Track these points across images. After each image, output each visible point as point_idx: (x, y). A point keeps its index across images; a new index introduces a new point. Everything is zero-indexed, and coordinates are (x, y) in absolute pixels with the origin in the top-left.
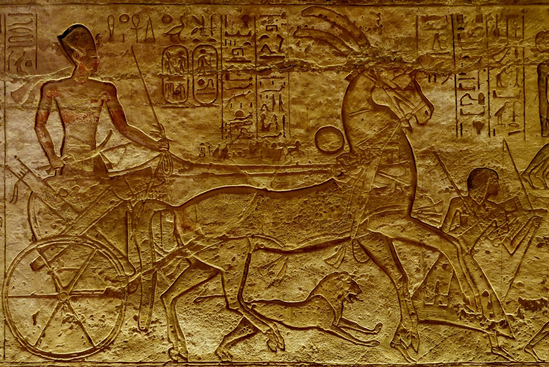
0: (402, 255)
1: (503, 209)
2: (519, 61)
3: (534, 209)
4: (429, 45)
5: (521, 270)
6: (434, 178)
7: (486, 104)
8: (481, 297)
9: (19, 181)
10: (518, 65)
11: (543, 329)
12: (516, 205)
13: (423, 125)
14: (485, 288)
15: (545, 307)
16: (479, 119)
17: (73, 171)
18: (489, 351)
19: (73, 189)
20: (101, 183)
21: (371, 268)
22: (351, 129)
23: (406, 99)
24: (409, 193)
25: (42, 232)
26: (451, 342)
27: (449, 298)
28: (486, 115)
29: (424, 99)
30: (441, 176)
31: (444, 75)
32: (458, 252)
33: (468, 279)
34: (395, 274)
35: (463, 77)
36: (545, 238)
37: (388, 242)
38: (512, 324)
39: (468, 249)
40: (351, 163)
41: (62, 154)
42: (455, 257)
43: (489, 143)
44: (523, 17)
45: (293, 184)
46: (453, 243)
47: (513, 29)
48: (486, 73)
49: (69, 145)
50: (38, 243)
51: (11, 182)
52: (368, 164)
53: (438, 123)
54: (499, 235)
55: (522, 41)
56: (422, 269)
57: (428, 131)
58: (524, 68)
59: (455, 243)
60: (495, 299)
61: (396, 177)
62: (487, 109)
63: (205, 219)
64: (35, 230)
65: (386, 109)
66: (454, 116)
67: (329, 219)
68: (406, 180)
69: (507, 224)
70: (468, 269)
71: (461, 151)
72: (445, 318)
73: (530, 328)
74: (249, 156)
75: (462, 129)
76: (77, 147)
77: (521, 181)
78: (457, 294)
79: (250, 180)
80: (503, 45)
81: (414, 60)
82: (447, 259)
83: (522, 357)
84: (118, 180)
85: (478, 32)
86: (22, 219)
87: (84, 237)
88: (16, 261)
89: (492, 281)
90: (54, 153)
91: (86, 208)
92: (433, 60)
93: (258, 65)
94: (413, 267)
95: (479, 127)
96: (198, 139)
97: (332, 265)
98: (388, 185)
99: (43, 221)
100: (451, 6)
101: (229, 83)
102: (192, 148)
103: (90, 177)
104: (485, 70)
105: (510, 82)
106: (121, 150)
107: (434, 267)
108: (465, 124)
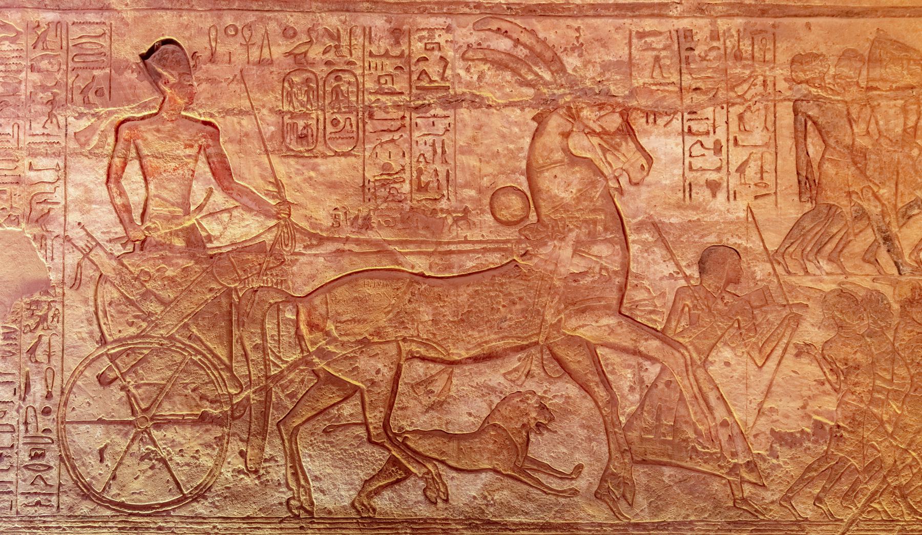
0: (610, 368)
3: (791, 303)
8: (719, 428)
9: (83, 258)
11: (804, 474)
12: (765, 298)
13: (637, 184)
17: (159, 245)
19: (158, 270)
20: (196, 263)
21: (568, 385)
22: (540, 190)
23: (616, 148)
24: (617, 280)
25: (113, 331)
29: (641, 149)
30: (663, 256)
32: (686, 366)
33: (701, 402)
34: (601, 392)
36: (806, 344)
37: (590, 348)
38: (762, 466)
40: (538, 237)
41: (142, 221)
43: (728, 211)
45: (460, 267)
46: (679, 352)
49: (152, 209)
50: (109, 347)
51: (73, 259)
52: (562, 239)
56: (638, 388)
59: (683, 351)
60: (738, 431)
61: (600, 257)
63: (339, 314)
64: (104, 327)
65: (589, 163)
67: (509, 316)
68: (615, 261)
70: (700, 389)
71: (690, 221)
72: (670, 456)
74: (400, 226)
75: (691, 190)
76: (164, 211)
77: (772, 264)
78: (686, 422)
79: (401, 259)
83: (776, 513)
84: (220, 259)
86: (87, 312)
87: (171, 338)
88: (77, 372)
89: (734, 405)
90: (132, 221)
91: (176, 298)
93: (412, 98)
94: (625, 385)
96: (332, 201)
97: (513, 381)
98: (590, 268)
99: (116, 315)
101: (373, 124)
102: (323, 217)
103: (181, 253)
106: (225, 217)
107: (654, 384)
108: (696, 184)
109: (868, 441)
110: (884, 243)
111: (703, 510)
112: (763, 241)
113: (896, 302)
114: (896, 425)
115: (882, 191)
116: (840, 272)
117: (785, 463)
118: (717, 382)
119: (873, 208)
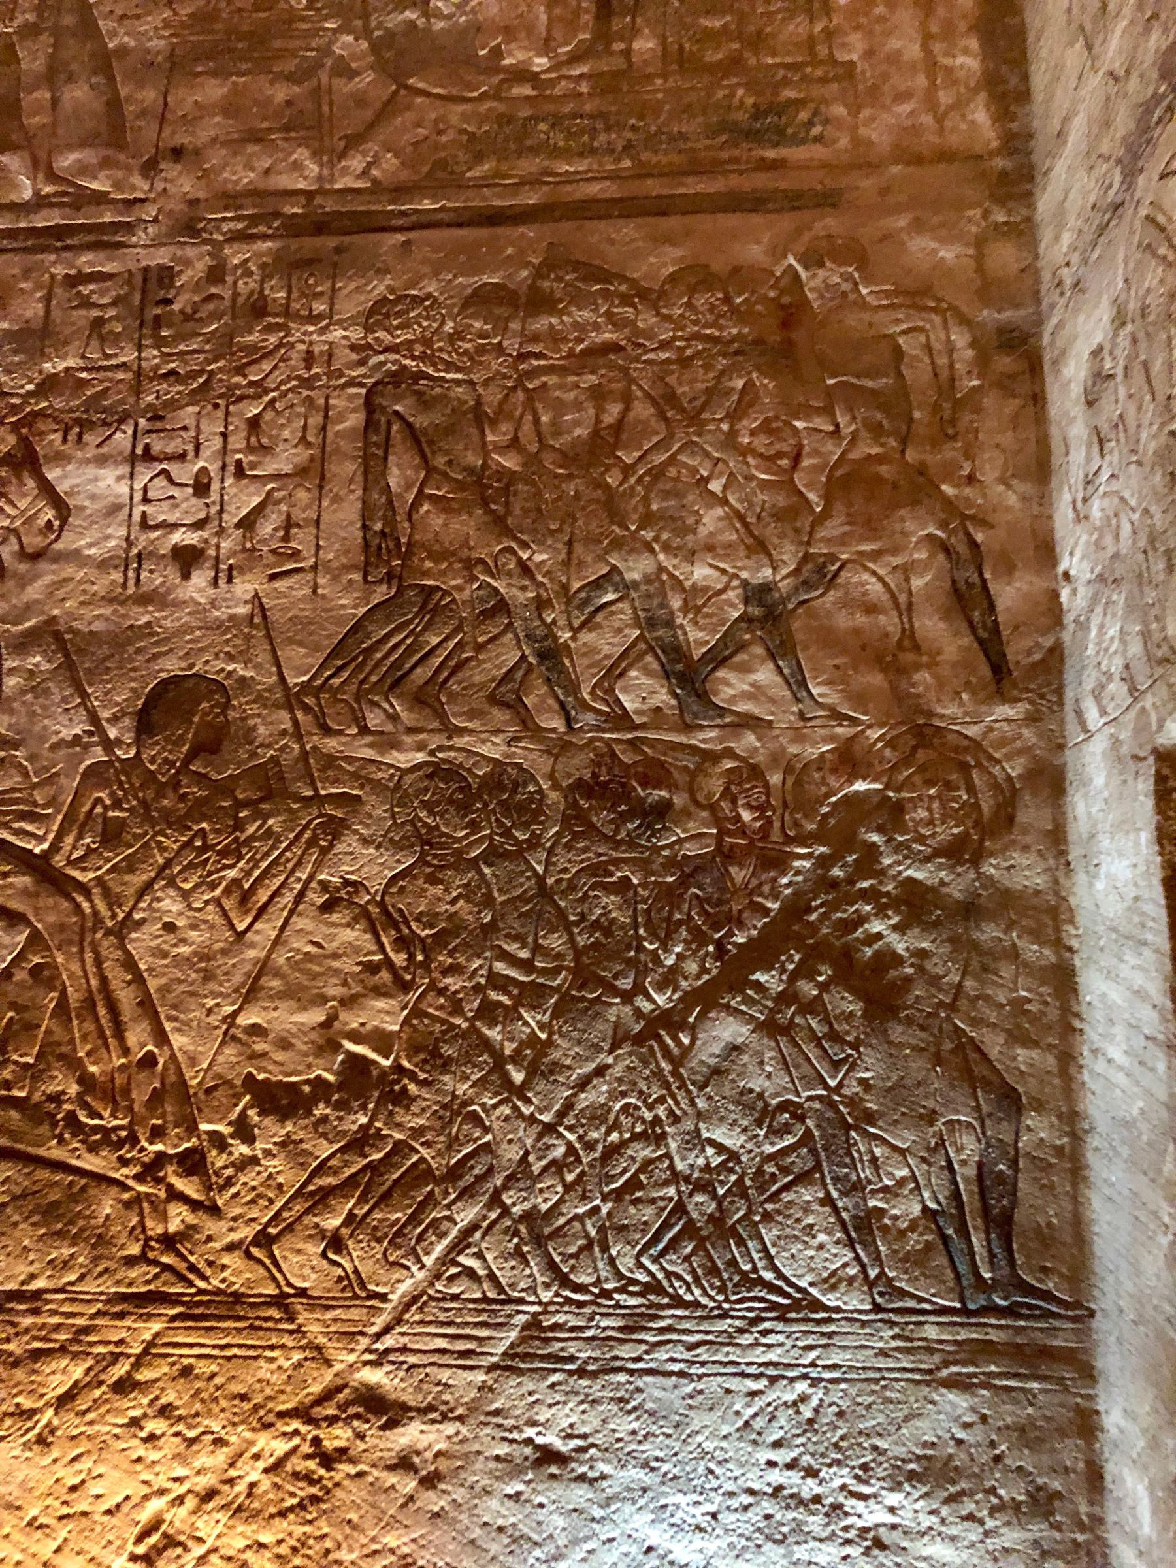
1: (231, 794)
2: (317, 377)
4: (75, 346)
5: (263, 981)
6: (45, 708)
7: (214, 496)
8: (134, 1070)
10: (312, 389)
13: (36, 556)
14: (150, 1040)
15: (321, 1105)
16: (192, 538)
18: (135, 1249)
26: (16, 1218)
27: (35, 1073)
28: (213, 527)
29: (47, 490)
30: (65, 700)
31: (105, 423)
33: (102, 1011)
35: (159, 425)
36: (347, 883)
39: (114, 916)
42: (70, 942)
44: (335, 265)
47: (303, 295)
48: (220, 414)
53: (77, 552)
54: (210, 874)
55: (327, 327)
57: (48, 574)
58: (327, 398)
59: (80, 899)
62: (214, 509)
66: (123, 532)
69: (236, 839)
70: (104, 981)
73: (270, 1176)
77: (292, 711)
78: (62, 1057)
80: (273, 340)
81: (30, 387)
82: (49, 949)
85: (211, 307)
89: (170, 1018)
92: (83, 383)
95: (187, 559)
100: (145, 246)
104: (216, 406)
105: (286, 433)
109: (465, 1104)
110: (540, 664)
111: (66, 1265)
112: (279, 666)
113: (556, 786)
114: (533, 1071)
115: (538, 558)
116: (435, 725)
117: (268, 1153)
118: (142, 966)
119: (519, 593)
